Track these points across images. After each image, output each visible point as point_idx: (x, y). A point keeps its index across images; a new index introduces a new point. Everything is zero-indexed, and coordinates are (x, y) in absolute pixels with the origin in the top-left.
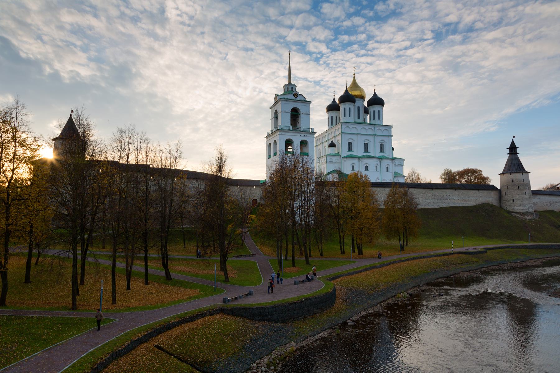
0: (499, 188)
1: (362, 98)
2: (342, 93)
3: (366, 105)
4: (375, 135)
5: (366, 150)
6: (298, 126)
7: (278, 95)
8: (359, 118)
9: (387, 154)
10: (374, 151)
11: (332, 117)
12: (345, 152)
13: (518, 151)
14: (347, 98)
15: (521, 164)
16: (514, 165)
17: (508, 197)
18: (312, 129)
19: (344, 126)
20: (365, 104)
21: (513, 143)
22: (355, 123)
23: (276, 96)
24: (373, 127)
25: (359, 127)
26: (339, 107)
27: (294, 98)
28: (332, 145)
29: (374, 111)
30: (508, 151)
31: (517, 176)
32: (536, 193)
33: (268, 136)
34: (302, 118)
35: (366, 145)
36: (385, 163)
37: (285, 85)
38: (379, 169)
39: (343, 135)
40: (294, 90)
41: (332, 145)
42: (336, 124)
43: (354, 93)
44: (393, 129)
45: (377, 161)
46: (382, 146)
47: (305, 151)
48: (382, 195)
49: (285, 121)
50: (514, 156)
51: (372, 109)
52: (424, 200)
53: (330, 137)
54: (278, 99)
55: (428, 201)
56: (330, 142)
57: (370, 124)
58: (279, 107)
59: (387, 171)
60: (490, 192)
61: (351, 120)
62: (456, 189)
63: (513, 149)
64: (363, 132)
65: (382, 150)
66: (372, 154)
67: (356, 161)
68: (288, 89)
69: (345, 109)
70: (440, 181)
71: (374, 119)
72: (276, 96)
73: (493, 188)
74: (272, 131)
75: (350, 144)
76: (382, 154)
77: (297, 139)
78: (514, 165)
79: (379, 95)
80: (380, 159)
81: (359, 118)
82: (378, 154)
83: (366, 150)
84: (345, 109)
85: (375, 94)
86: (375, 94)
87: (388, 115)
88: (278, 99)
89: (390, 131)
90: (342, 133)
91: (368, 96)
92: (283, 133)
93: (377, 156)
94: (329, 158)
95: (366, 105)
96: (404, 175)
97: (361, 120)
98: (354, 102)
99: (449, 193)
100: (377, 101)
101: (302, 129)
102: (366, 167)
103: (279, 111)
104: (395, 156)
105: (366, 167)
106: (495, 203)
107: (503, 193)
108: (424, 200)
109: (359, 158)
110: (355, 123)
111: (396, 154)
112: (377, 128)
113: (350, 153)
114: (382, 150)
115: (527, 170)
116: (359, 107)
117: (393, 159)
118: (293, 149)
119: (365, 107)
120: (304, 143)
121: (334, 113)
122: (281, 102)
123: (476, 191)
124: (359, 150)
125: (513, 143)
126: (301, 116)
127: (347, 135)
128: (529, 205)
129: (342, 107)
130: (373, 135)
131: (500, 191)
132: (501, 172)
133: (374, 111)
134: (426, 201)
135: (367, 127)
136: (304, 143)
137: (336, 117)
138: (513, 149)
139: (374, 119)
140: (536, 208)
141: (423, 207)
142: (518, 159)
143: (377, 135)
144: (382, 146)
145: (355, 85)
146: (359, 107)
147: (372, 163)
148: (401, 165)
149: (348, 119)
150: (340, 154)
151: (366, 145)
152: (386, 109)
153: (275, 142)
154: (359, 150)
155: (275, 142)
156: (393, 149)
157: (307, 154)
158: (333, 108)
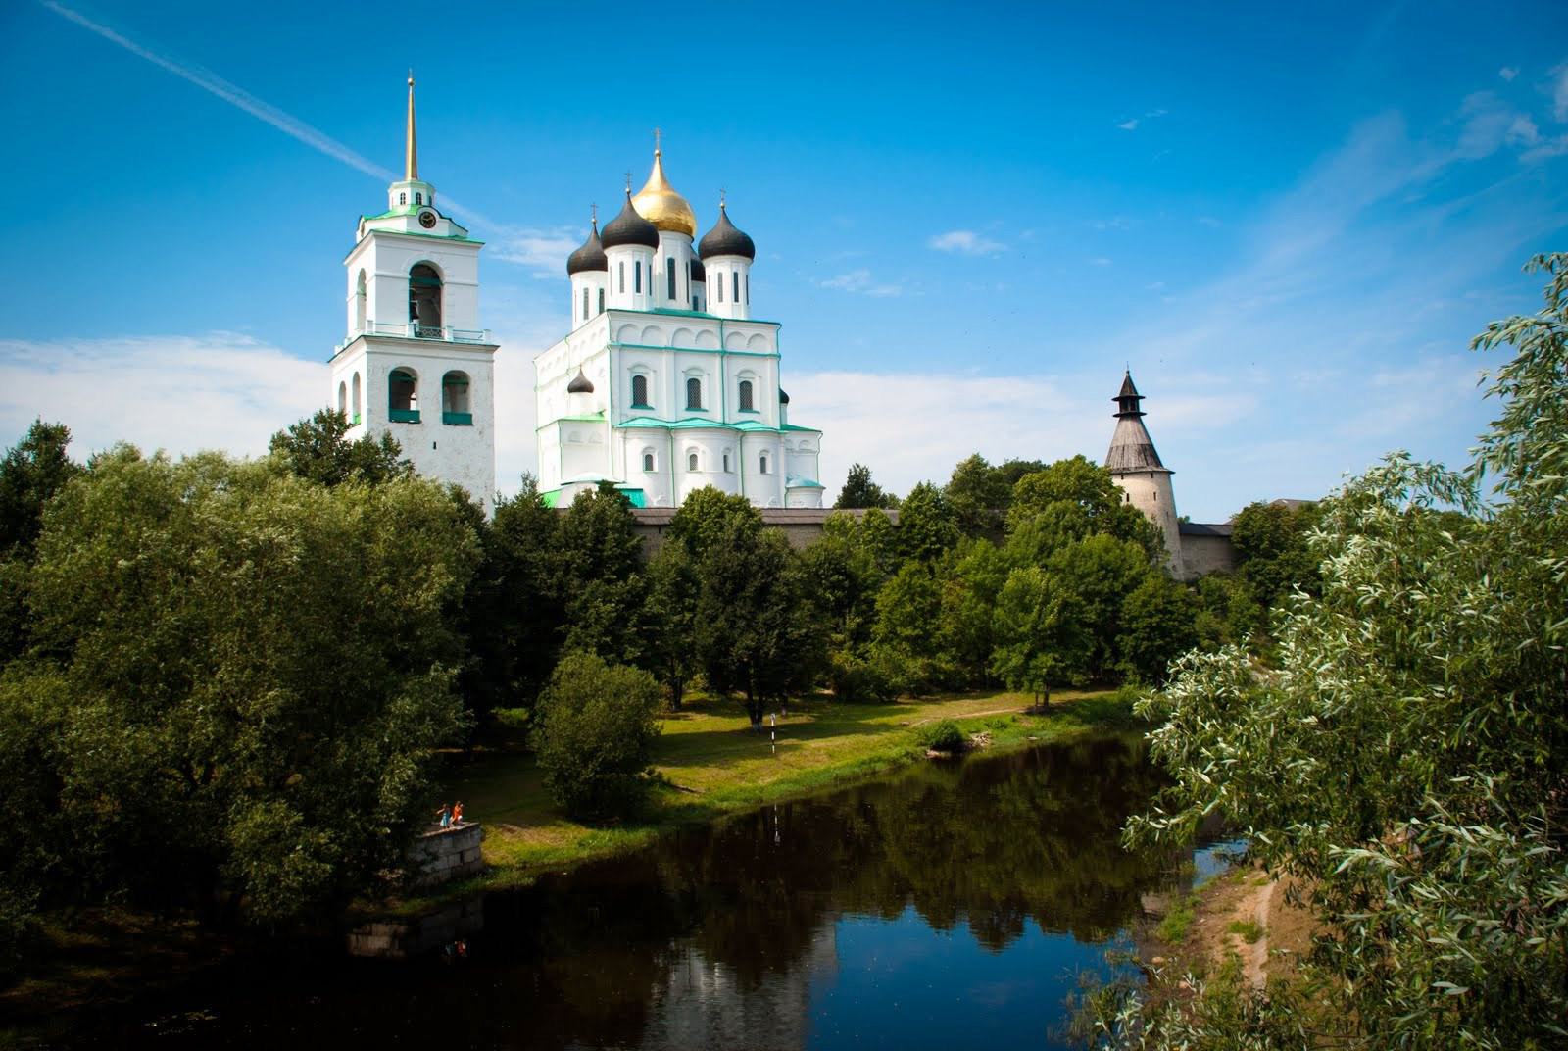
5: (694, 402)
8: (672, 295)
13: (1143, 406)
21: (1129, 384)
22: (659, 312)
24: (714, 328)
27: (422, 230)
28: (581, 387)
30: (1116, 407)
35: (693, 386)
40: (425, 201)
42: (601, 310)
56: (574, 376)
59: (763, 470)
64: (686, 341)
65: (746, 404)
69: (622, 264)
71: (721, 299)
76: (746, 416)
84: (622, 264)
91: (704, 227)
92: (383, 349)
103: (370, 274)
110: (659, 312)
115: (1167, 465)
125: (1129, 384)
126: (446, 286)
130: (715, 352)
135: (696, 327)
137: (602, 292)
143: (731, 353)
151: (693, 386)
153: (356, 378)
155: (356, 378)
157: (466, 420)
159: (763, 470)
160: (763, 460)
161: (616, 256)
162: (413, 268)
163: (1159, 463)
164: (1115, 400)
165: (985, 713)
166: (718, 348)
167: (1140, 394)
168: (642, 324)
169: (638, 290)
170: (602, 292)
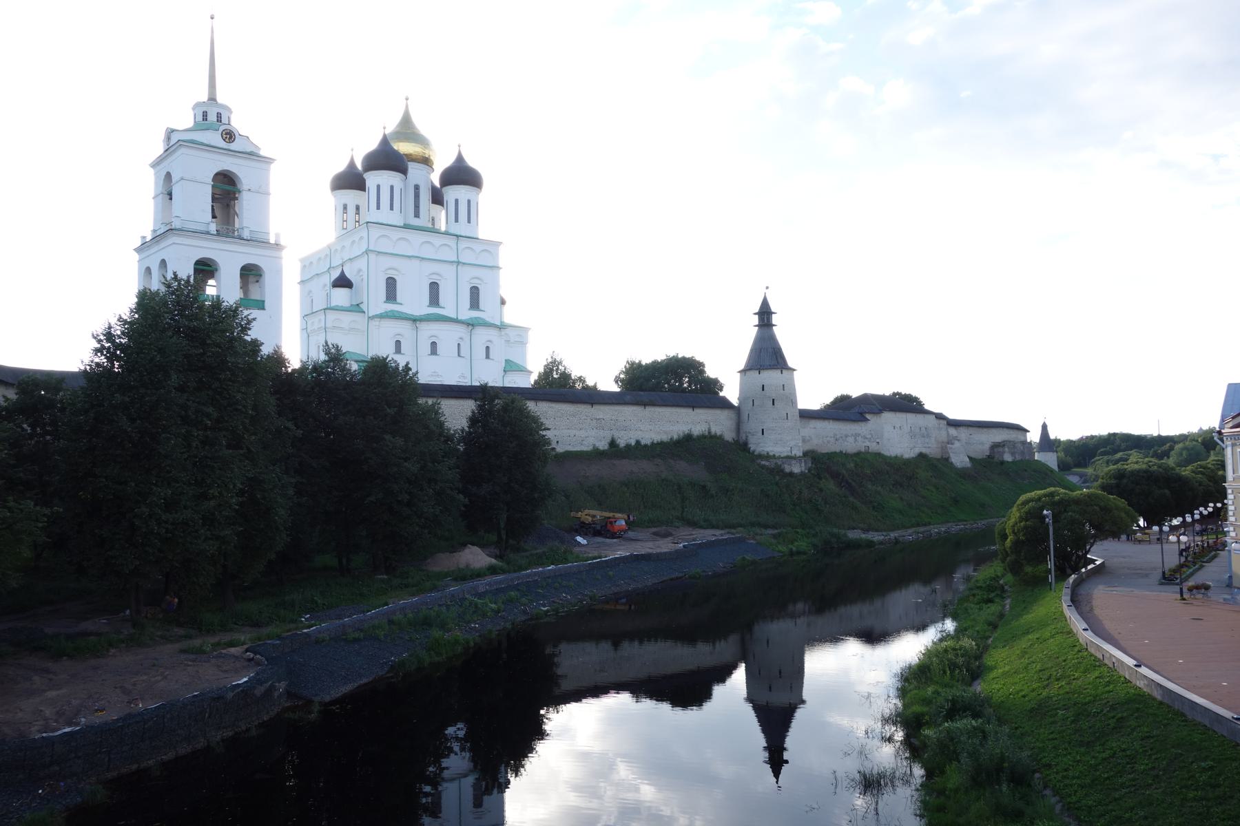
0: (735, 402)
1: (426, 161)
2: (372, 144)
3: (437, 184)
4: (458, 263)
5: (434, 299)
6: (237, 225)
7: (173, 131)
8: (417, 215)
9: (488, 311)
10: (454, 303)
11: (345, 207)
12: (376, 302)
14: (387, 159)
15: (780, 349)
16: (767, 355)
17: (752, 426)
18: (277, 235)
19: (375, 232)
20: (436, 179)
21: (765, 304)
23: (170, 132)
24: (451, 242)
25: (417, 238)
26: (364, 181)
28: (343, 282)
29: (457, 201)
30: (756, 320)
31: (771, 377)
32: (806, 415)
33: (143, 248)
34: (246, 204)
35: (434, 288)
36: (482, 336)
37: (197, 105)
38: (465, 351)
39: (372, 256)
40: (224, 120)
41: (343, 282)
43: (403, 148)
44: (501, 247)
45: (460, 331)
46: (475, 292)
47: (255, 295)
48: (456, 416)
49: (197, 204)
51: (451, 193)
52: (572, 432)
53: (337, 262)
54: (174, 143)
55: (582, 434)
56: (336, 274)
57: (446, 233)
58: (177, 166)
59: (488, 357)
60: (718, 412)
61: (395, 218)
62: (645, 405)
63: (765, 315)
64: (428, 252)
65: (475, 303)
66: (448, 309)
67: (404, 329)
68: (205, 115)
69: (378, 187)
70: (615, 388)
71: (457, 220)
72: (170, 132)
73: (725, 404)
74: (154, 231)
75: (391, 284)
76: (475, 314)
77: (230, 259)
78: (767, 355)
79: (472, 162)
80: (471, 324)
81: (417, 215)
82: (466, 314)
83: (434, 299)
84: (378, 187)
85: (460, 159)
86: (460, 159)
87: (492, 212)
88: (173, 141)
89: (495, 256)
90: (367, 252)
91: (442, 161)
93: (461, 317)
94: (332, 316)
95: (437, 184)
96: (529, 368)
97: (423, 222)
98: (404, 171)
99: (629, 413)
100: (462, 175)
101: (246, 234)
102: (434, 344)
103: (175, 178)
104: (508, 319)
105: (434, 344)
106: (729, 436)
107: (745, 417)
108: (572, 432)
109: (415, 320)
110: (406, 227)
111: (510, 316)
112: (463, 244)
113: (391, 307)
114: (475, 303)
115: (790, 364)
116: (417, 188)
117: (502, 327)
118: (218, 286)
119: (434, 189)
120: (250, 274)
121: (351, 196)
122: (183, 150)
123: (690, 411)
124: (413, 300)
125: (765, 304)
127: (382, 258)
128: (792, 443)
129: (372, 179)
131: (737, 410)
132: (742, 367)
133: (457, 201)
134: (578, 433)
135: (437, 240)
136: (250, 274)
138: (765, 315)
139: (457, 220)
140: (808, 447)
141: (571, 448)
144: (475, 292)
145: (407, 129)
146: (417, 188)
147: (448, 336)
148: (522, 343)
149: (385, 215)
150: (364, 307)
151: (434, 288)
152: (486, 199)
154: (413, 300)
156: (503, 302)
158: (350, 181)
159: (488, 357)
161: (372, 179)
162: (217, 174)
165: (665, 546)
166: (455, 259)
168: (396, 234)
169: (392, 209)
170: (358, 208)
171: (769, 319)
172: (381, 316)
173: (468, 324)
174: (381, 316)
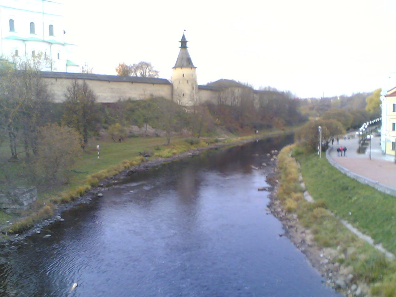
4: (44, 13)
13: (188, 45)
16: (185, 61)
21: (184, 37)
30: (180, 44)
31: (186, 71)
35: (32, 24)
36: (56, 49)
50: (184, 50)
63: (184, 43)
65: (51, 33)
78: (185, 61)
82: (48, 38)
93: (46, 39)
113: (12, 33)
114: (51, 33)
115: (195, 66)
132: (174, 66)
138: (184, 43)
142: (187, 54)
160: (58, 54)
163: (192, 64)
164: (179, 42)
167: (187, 41)
171: (185, 45)
172: (8, 38)
173: (49, 43)
174: (8, 38)
